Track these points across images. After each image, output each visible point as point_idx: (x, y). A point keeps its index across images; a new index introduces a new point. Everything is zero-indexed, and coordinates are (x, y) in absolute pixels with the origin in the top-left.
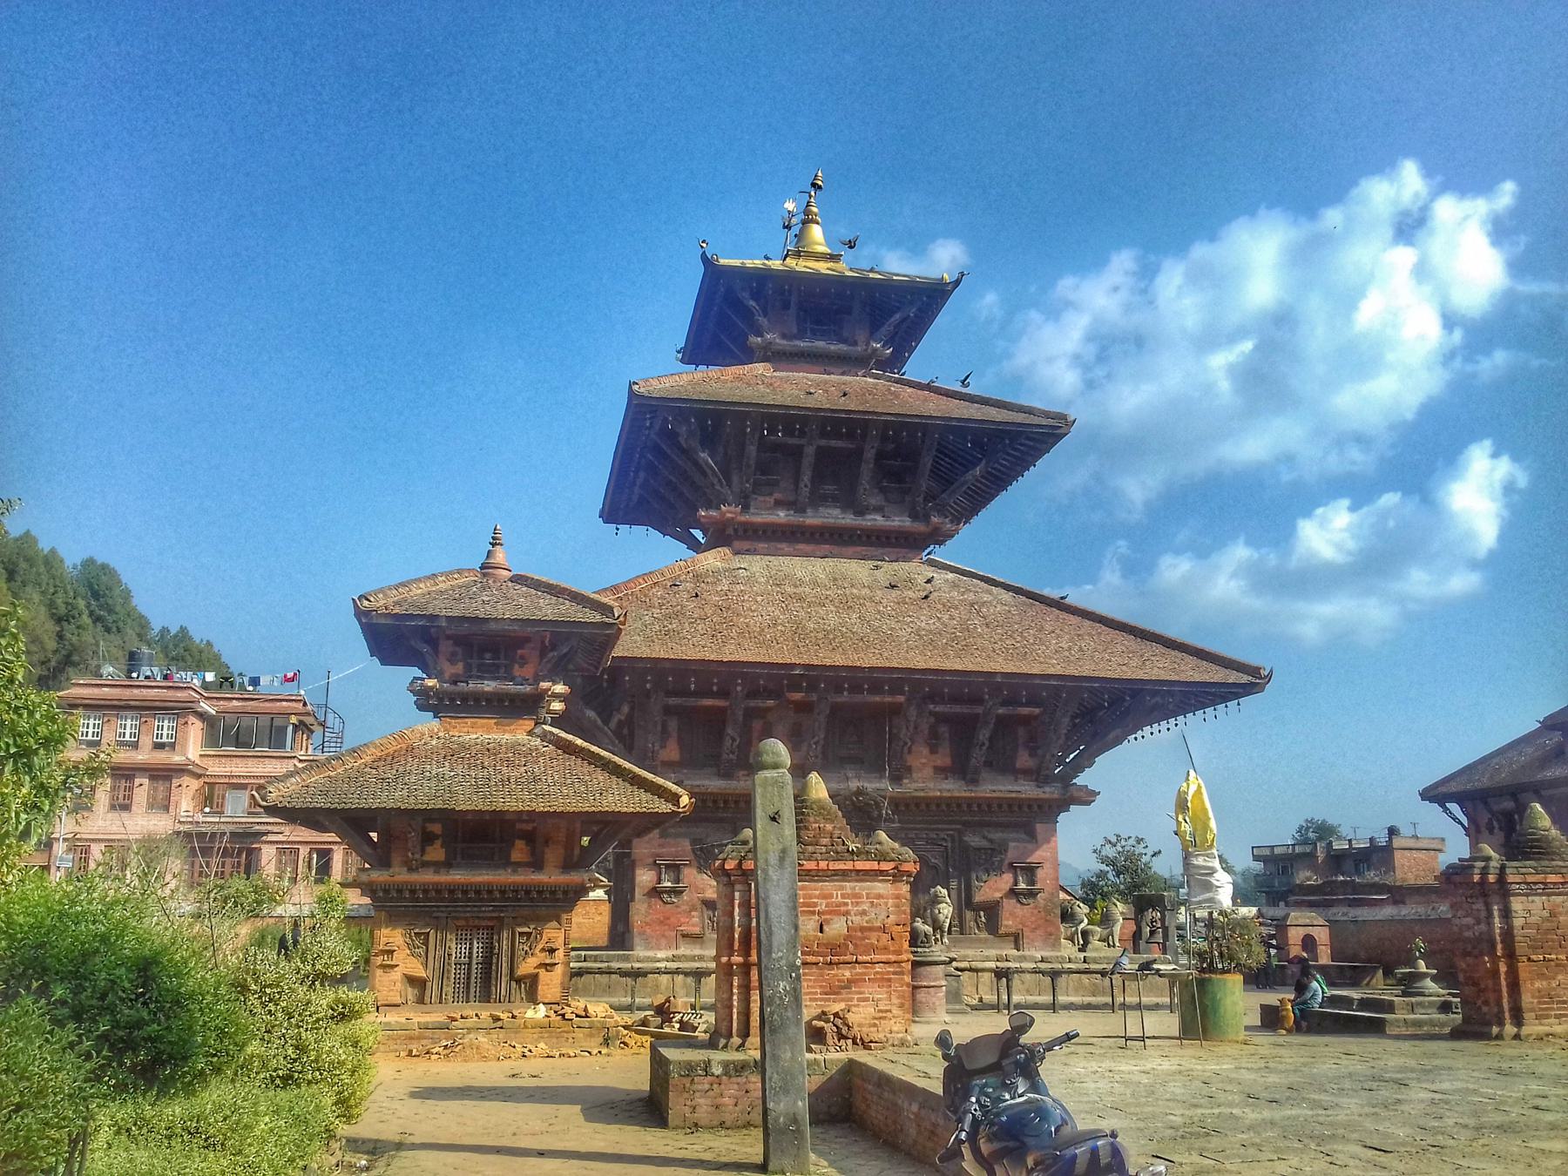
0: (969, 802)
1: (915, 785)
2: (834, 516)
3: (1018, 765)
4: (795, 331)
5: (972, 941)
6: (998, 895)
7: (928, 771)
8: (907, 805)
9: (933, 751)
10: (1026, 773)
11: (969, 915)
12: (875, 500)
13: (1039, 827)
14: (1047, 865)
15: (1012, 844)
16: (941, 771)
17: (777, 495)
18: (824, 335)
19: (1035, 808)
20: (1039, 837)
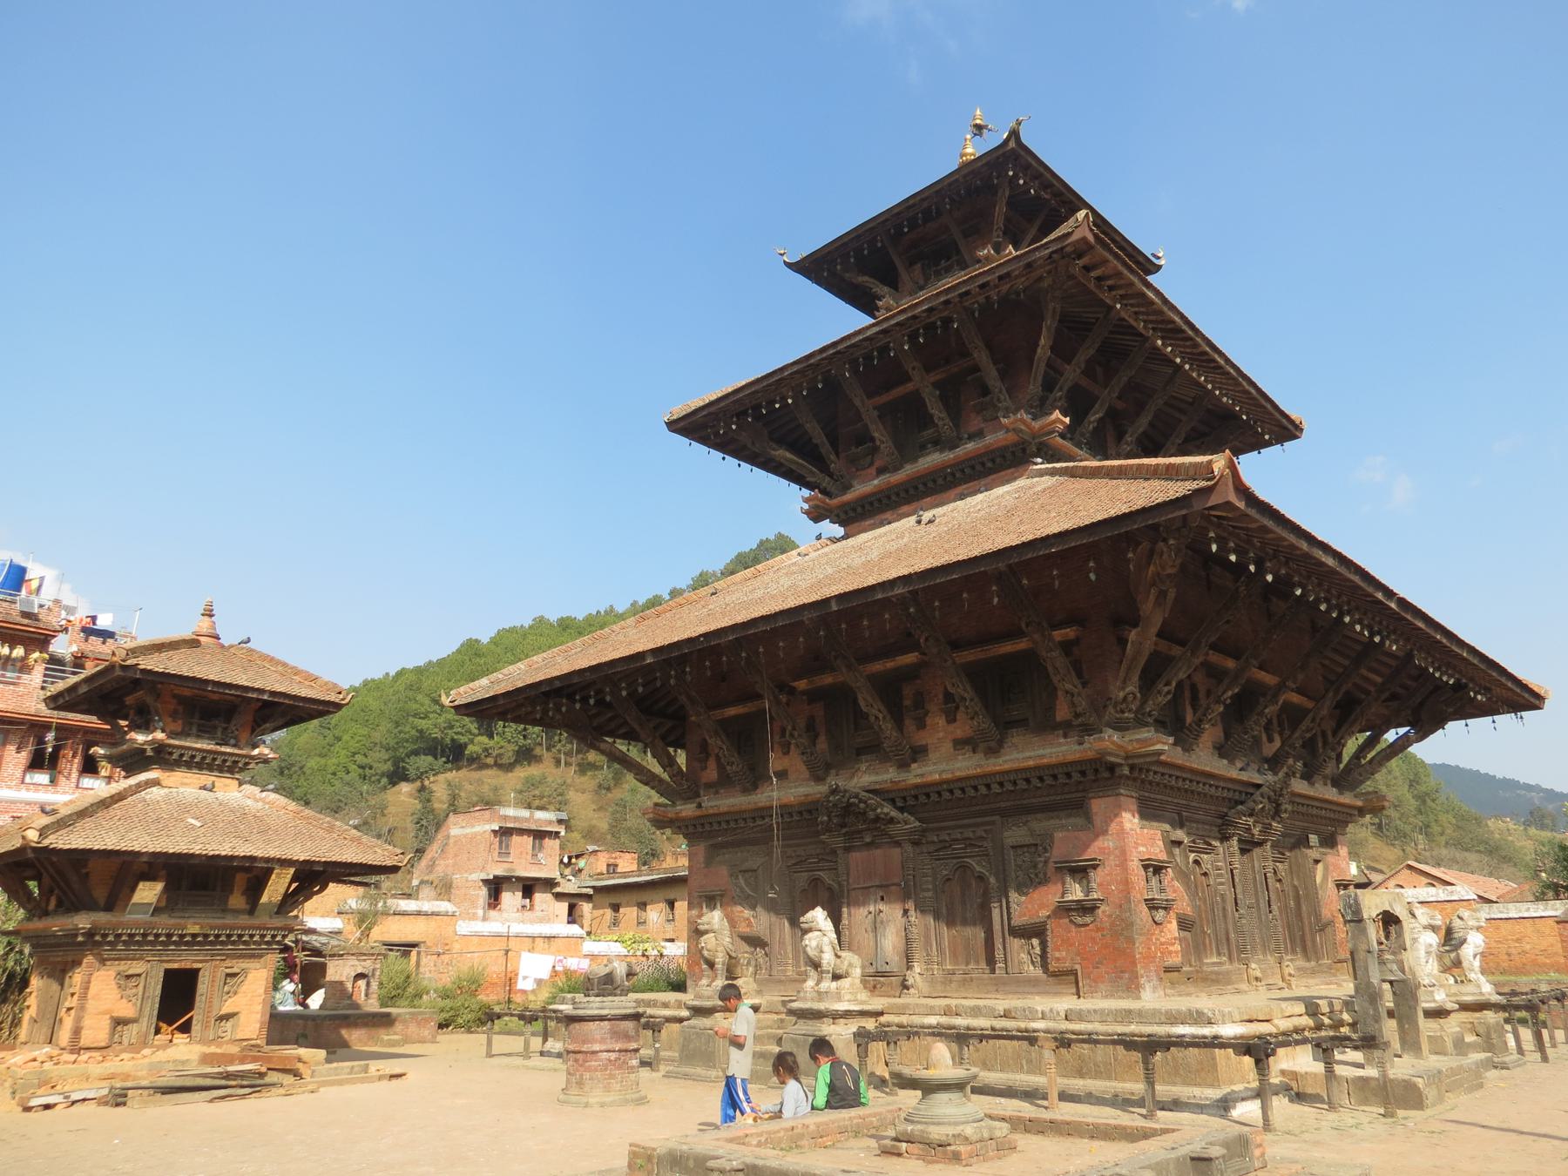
0: (987, 780)
1: (924, 769)
2: (932, 460)
3: (1058, 719)
4: (921, 282)
5: (1018, 982)
6: (1044, 913)
7: (948, 746)
8: (916, 797)
9: (951, 720)
10: (1066, 728)
11: (1016, 943)
12: (975, 423)
13: (1098, 806)
14: (1111, 862)
15: (1058, 835)
16: (959, 744)
17: (878, 463)
18: (948, 271)
19: (1076, 777)
20: (1098, 820)
